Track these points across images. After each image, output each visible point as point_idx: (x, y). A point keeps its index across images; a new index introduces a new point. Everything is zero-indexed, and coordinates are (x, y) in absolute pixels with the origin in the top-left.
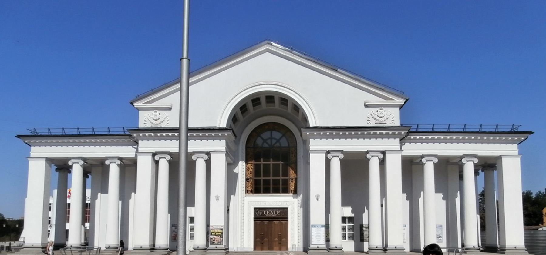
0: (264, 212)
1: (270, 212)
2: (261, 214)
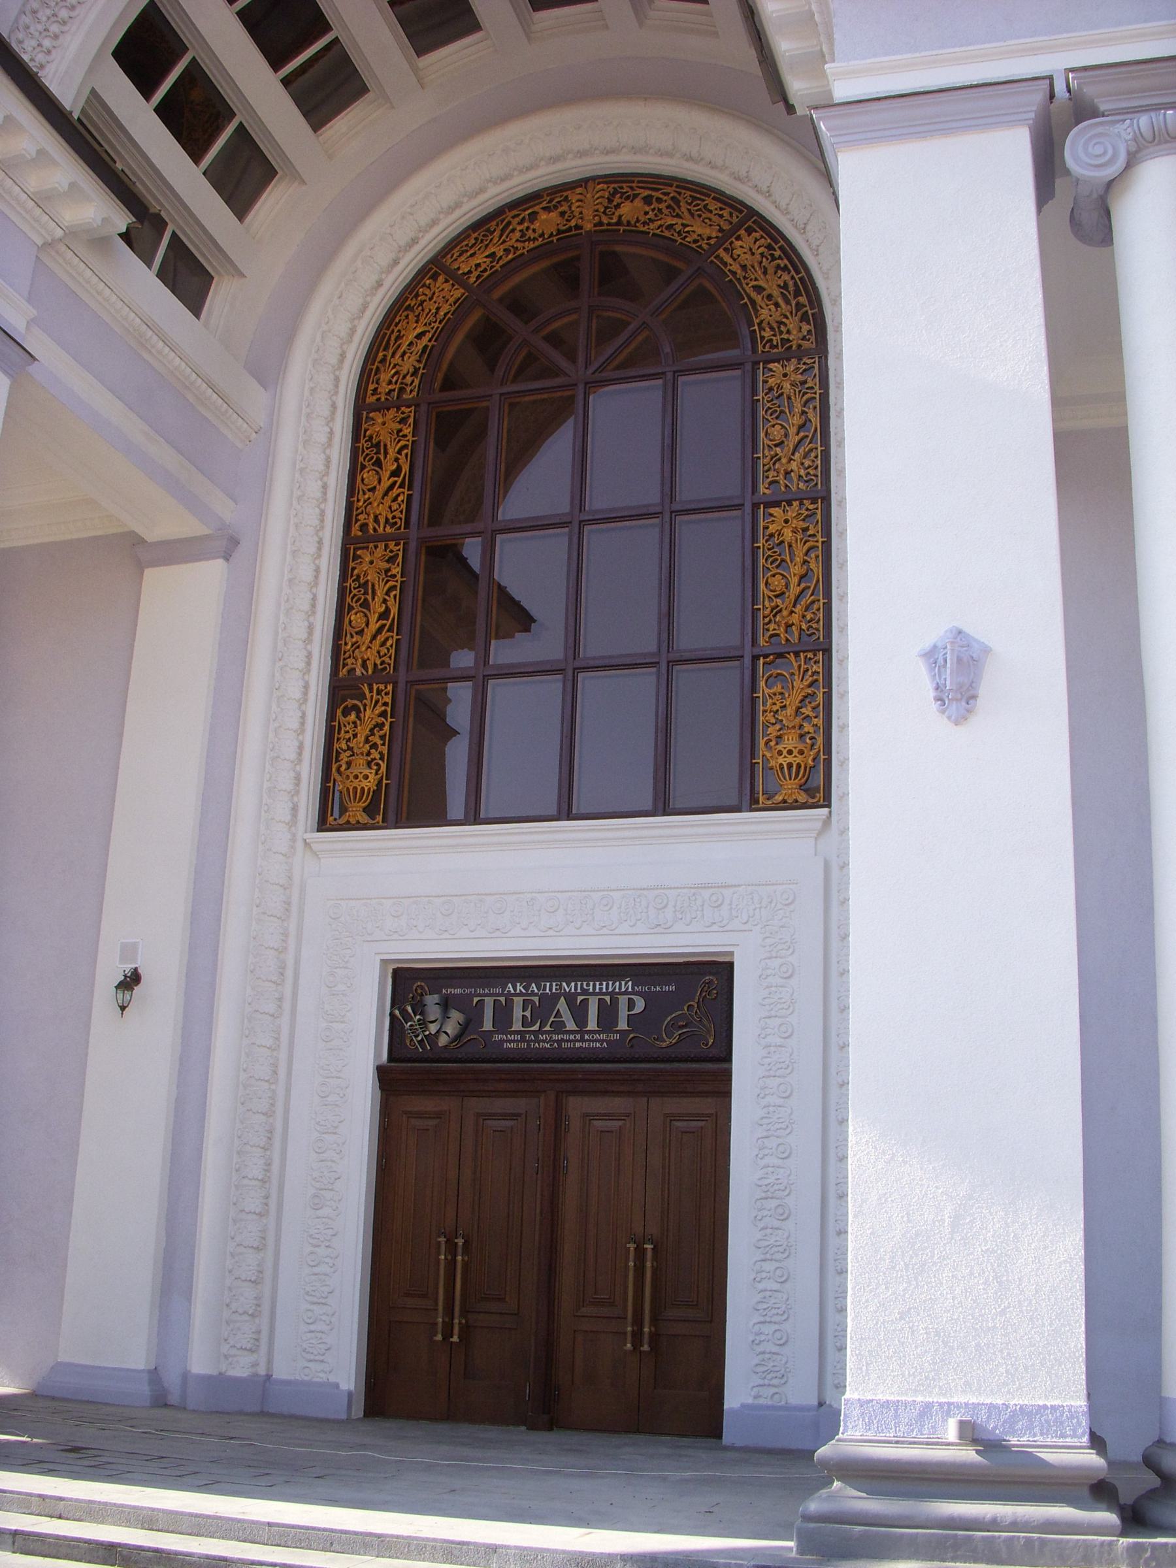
0: (489, 1002)
1: (543, 1009)
2: (451, 1028)
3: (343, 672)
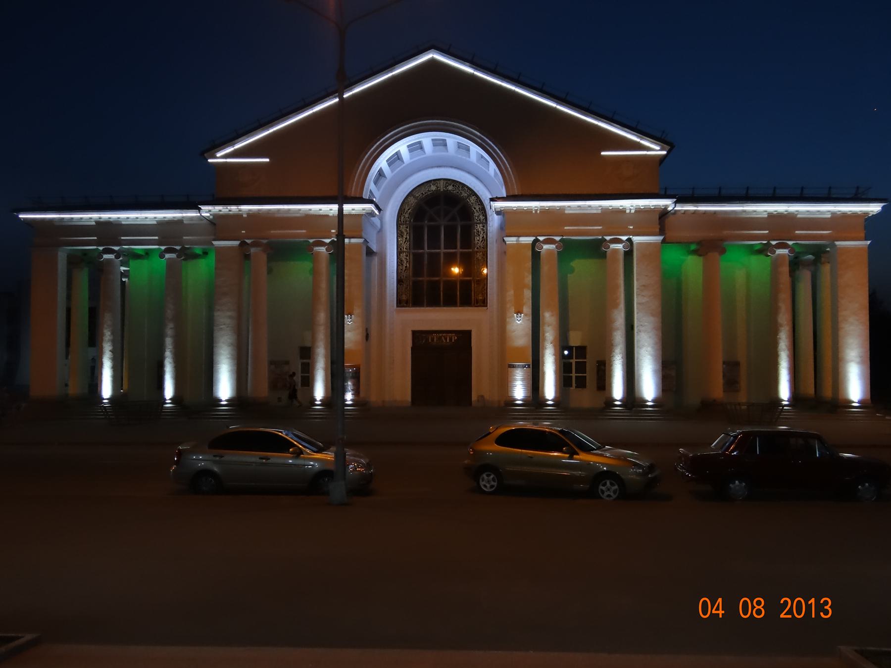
0: (430, 337)
1: (440, 338)
2: (424, 341)
3: (399, 278)
